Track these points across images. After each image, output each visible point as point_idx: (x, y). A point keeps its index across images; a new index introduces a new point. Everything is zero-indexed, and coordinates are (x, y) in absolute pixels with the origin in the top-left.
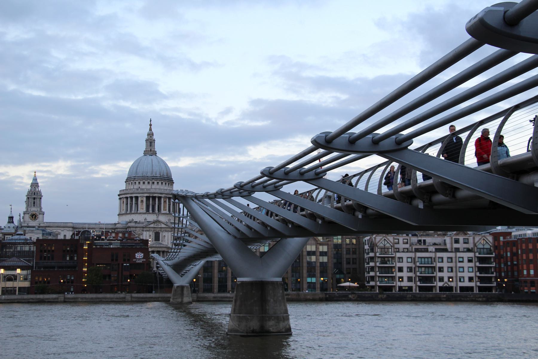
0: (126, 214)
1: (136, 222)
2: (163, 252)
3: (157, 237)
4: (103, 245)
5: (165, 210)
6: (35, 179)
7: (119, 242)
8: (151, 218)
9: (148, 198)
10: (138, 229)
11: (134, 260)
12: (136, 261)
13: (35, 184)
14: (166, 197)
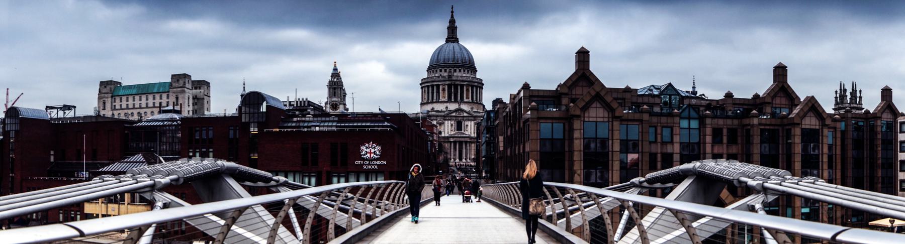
0: (428, 103)
1: (437, 111)
2: (466, 142)
3: (459, 127)
4: (299, 127)
5: (467, 98)
6: (335, 69)
7: (336, 119)
8: (453, 107)
9: (449, 86)
10: (439, 118)
11: (358, 162)
12: (361, 165)
13: (336, 74)
14: (467, 86)
